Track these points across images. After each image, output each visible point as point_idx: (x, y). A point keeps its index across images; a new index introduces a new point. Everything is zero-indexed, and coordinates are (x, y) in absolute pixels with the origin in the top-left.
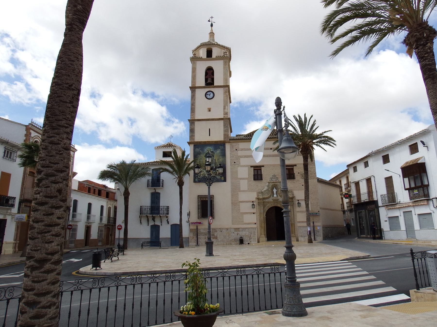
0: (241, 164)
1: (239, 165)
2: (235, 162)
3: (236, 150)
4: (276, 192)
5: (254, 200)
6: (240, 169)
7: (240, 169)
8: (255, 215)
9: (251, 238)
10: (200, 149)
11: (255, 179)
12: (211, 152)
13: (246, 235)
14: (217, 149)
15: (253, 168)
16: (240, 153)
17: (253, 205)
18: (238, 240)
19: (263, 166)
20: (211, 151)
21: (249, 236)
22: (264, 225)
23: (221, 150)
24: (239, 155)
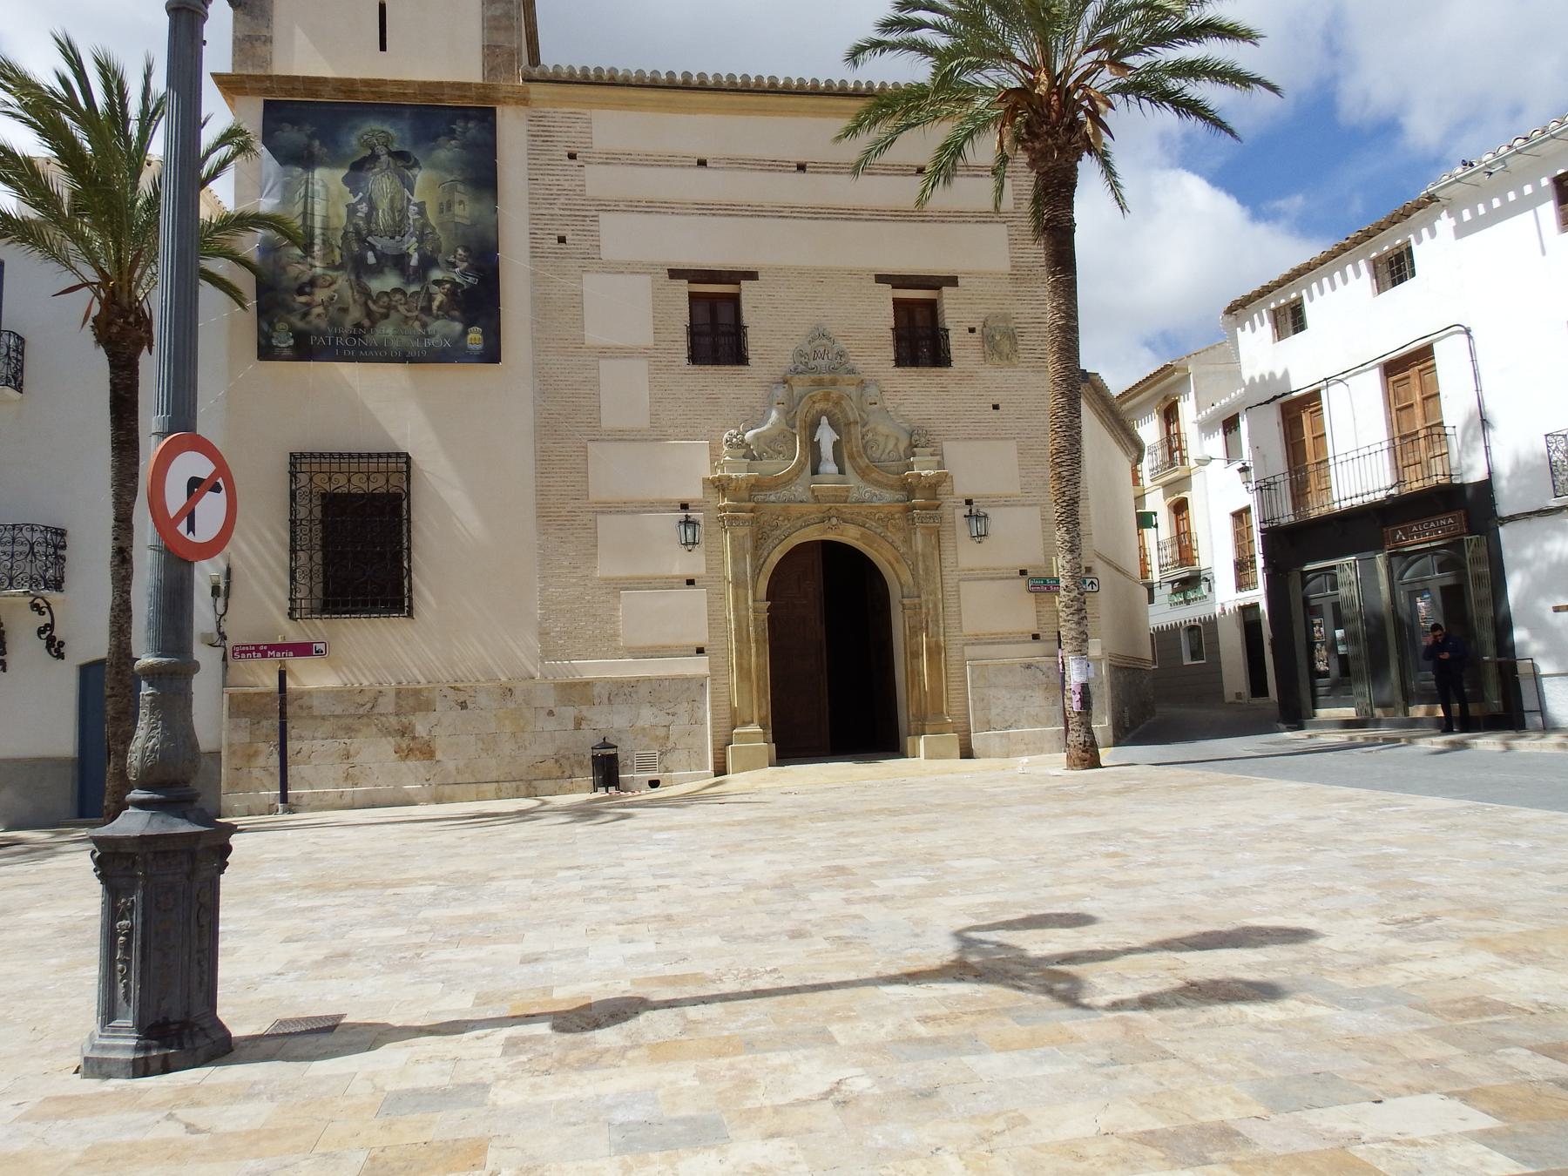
0: (609, 252)
1: (592, 259)
2: (562, 240)
3: (572, 156)
4: (837, 446)
5: (694, 493)
6: (594, 286)
7: (594, 286)
8: (698, 595)
9: (670, 745)
10: (308, 129)
11: (696, 357)
12: (391, 154)
13: (640, 723)
14: (435, 138)
15: (683, 288)
16: (599, 181)
17: (687, 522)
18: (580, 764)
19: (752, 275)
20: (395, 147)
21: (661, 732)
22: (759, 659)
23: (464, 147)
24: (590, 192)
